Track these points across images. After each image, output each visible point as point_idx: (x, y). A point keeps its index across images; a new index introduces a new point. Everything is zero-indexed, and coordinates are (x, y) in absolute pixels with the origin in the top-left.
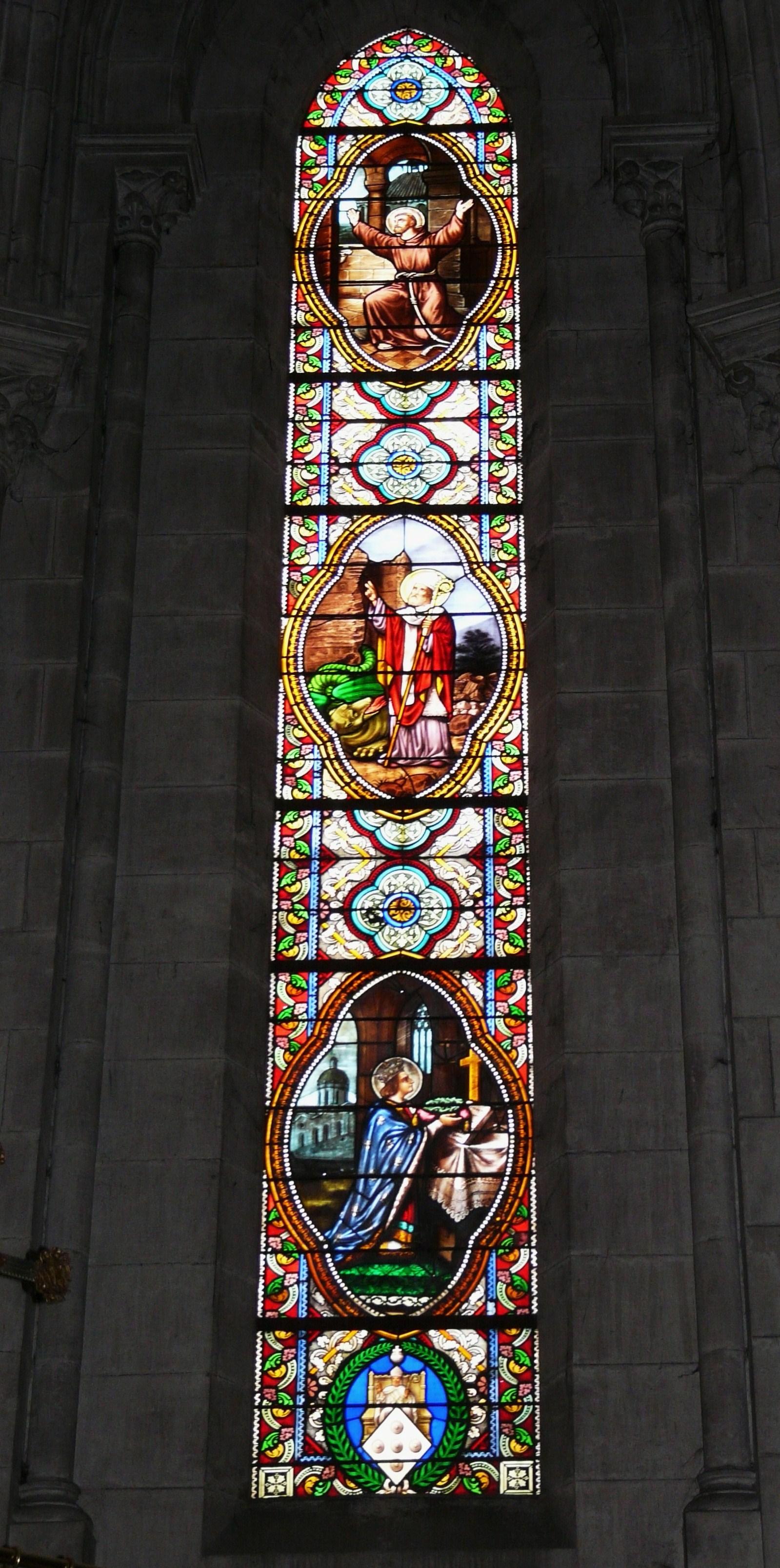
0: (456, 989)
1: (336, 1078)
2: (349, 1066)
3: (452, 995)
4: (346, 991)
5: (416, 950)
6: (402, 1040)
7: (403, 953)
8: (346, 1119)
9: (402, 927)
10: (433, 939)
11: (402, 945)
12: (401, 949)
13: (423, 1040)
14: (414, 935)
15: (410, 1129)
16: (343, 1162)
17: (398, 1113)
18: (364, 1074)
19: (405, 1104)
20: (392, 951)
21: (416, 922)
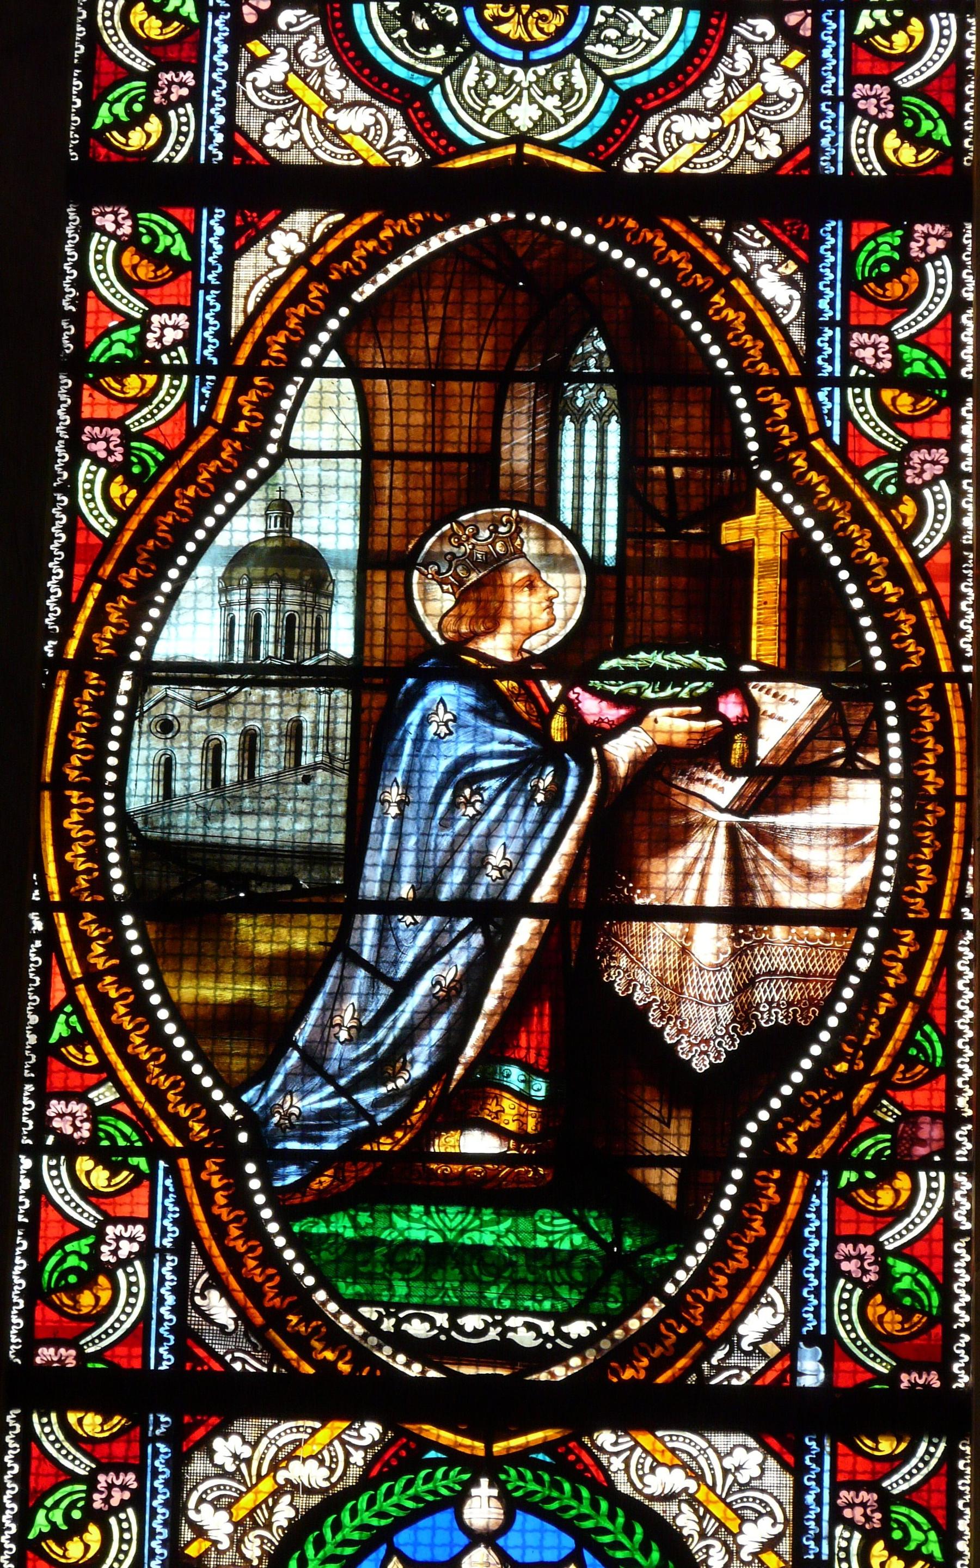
0: (714, 281)
1: (289, 562)
2: (331, 523)
3: (698, 302)
4: (322, 273)
6: (518, 452)
7: (529, 150)
8: (325, 714)
9: (526, 64)
10: (635, 107)
11: (524, 124)
12: (521, 139)
13: (591, 455)
14: (567, 93)
15: (545, 753)
16: (315, 855)
17: (499, 693)
18: (384, 559)
19: (526, 668)
20: (490, 144)
21: (577, 48)
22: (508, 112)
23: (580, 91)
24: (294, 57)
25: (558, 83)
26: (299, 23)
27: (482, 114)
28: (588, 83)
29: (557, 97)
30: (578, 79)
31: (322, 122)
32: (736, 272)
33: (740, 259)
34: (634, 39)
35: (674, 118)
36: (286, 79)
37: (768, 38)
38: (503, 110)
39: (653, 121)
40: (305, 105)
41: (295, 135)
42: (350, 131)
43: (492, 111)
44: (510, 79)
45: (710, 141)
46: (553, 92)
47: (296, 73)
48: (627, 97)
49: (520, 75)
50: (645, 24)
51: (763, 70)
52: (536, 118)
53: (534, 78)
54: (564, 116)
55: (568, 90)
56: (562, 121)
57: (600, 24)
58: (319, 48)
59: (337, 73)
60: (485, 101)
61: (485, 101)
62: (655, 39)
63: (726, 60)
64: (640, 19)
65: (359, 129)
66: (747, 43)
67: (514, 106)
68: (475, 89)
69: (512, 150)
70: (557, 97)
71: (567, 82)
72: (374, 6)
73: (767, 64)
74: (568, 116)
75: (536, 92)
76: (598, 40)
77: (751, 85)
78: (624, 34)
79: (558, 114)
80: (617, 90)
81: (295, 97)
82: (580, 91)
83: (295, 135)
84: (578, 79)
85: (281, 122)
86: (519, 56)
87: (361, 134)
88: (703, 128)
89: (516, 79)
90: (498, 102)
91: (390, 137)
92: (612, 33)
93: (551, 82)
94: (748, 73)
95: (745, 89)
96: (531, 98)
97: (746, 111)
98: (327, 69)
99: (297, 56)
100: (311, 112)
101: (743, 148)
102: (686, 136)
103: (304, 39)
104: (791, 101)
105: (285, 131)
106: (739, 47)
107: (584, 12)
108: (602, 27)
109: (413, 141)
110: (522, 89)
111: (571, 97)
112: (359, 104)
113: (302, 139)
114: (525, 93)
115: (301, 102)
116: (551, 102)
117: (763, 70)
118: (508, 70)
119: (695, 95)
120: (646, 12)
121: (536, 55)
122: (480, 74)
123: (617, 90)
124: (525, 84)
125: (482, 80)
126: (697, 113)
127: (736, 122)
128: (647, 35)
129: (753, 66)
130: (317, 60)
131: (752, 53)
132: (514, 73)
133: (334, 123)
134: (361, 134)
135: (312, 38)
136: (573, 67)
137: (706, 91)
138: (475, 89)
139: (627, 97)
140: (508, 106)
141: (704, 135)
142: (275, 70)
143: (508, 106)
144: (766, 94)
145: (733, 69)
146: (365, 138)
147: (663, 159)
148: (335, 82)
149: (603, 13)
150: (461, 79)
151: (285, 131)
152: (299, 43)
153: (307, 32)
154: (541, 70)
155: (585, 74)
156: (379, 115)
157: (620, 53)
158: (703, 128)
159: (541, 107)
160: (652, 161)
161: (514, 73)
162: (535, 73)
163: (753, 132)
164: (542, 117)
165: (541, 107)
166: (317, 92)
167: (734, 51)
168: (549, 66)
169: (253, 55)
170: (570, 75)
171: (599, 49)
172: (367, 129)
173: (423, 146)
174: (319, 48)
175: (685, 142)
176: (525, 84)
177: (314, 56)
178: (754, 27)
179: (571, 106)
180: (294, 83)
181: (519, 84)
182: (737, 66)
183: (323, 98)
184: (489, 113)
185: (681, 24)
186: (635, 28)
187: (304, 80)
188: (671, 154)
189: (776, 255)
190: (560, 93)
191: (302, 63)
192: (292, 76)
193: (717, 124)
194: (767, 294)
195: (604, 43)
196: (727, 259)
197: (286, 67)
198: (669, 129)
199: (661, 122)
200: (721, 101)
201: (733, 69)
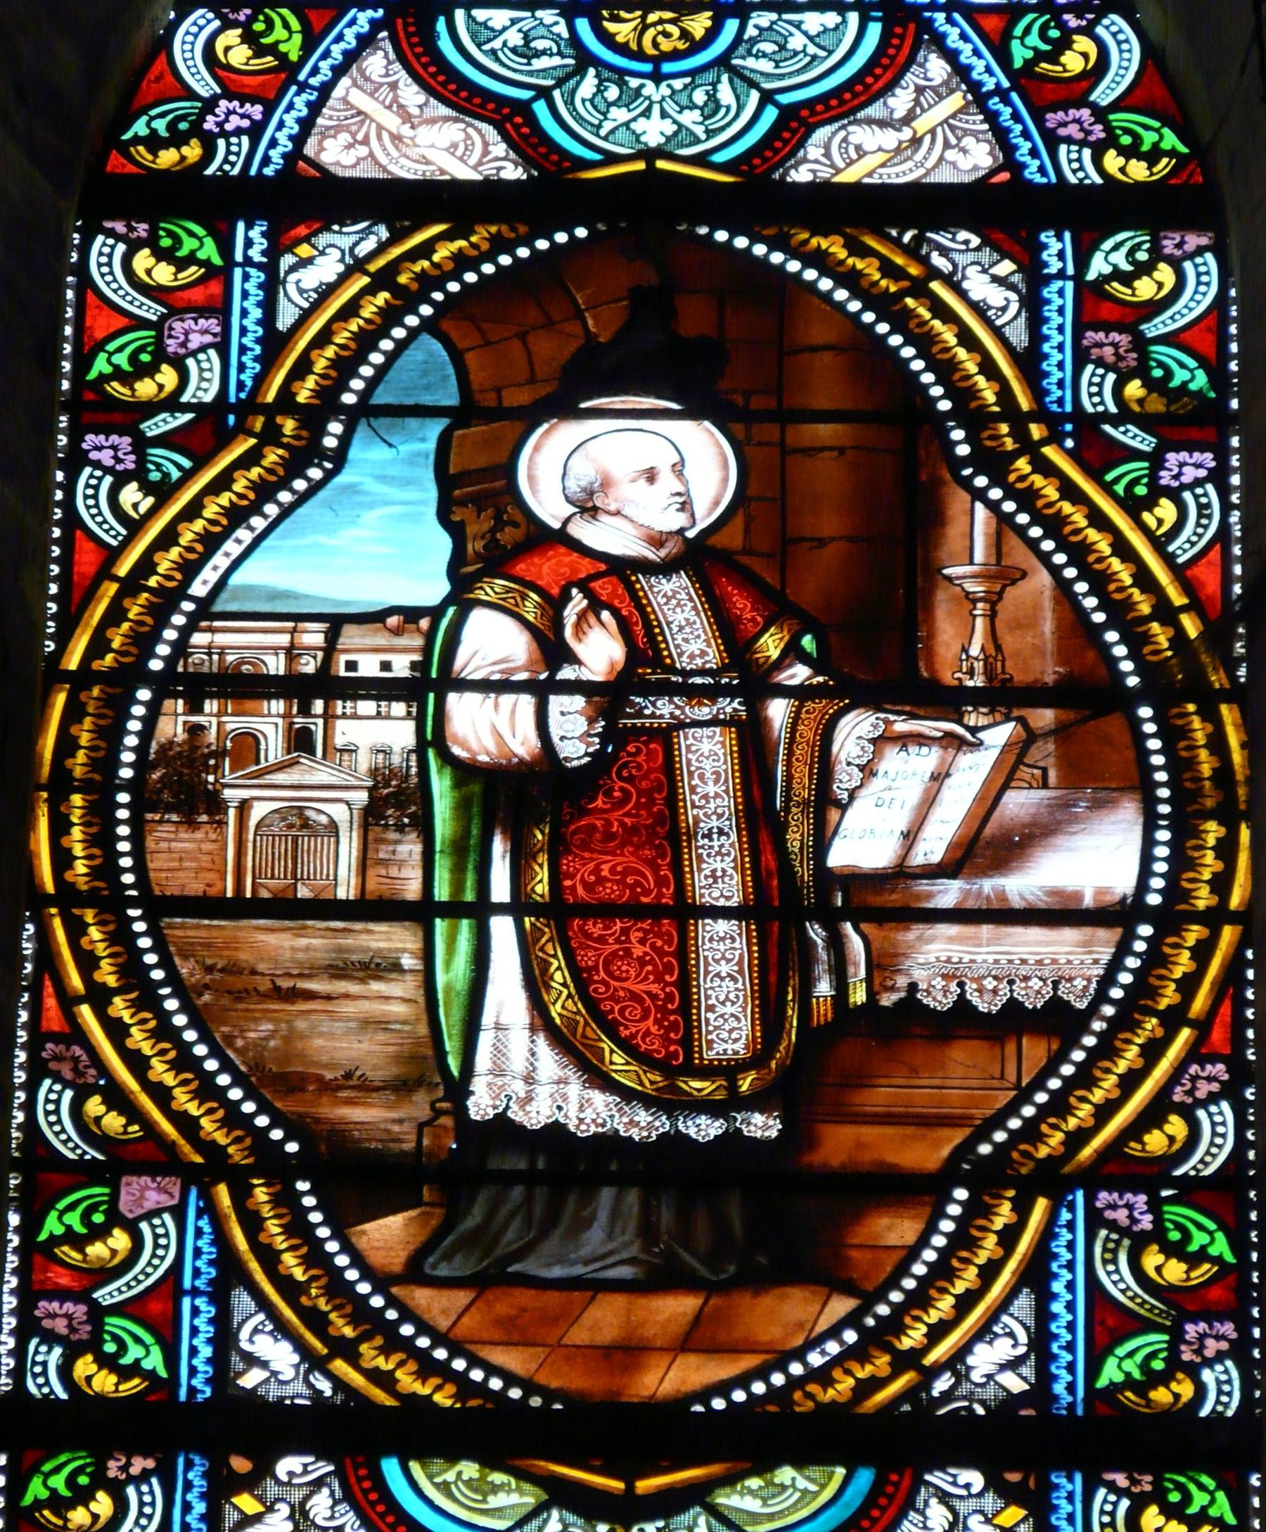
5: (719, 158)
7: (661, 164)
9: (657, 77)
12: (649, 155)
14: (712, 106)
21: (723, 61)
22: (633, 125)
23: (728, 108)
25: (699, 97)
27: (599, 127)
28: (738, 98)
29: (698, 112)
30: (725, 94)
32: (935, 273)
33: (937, 260)
34: (796, 53)
35: (850, 128)
38: (627, 124)
39: (821, 134)
40: (372, 120)
41: (362, 151)
42: (432, 146)
43: (614, 124)
44: (638, 92)
46: (693, 106)
48: (787, 113)
49: (650, 88)
50: (811, 39)
52: (669, 133)
53: (668, 92)
54: (707, 131)
55: (711, 105)
56: (703, 136)
57: (751, 38)
58: (390, 63)
59: (415, 88)
60: (604, 114)
61: (604, 114)
62: (824, 54)
64: (805, 33)
67: (642, 120)
68: (592, 101)
69: (640, 166)
70: (698, 112)
71: (712, 97)
72: (460, 15)
74: (710, 133)
75: (670, 107)
76: (749, 53)
78: (782, 48)
79: (699, 131)
80: (777, 104)
82: (728, 108)
83: (362, 151)
84: (725, 94)
85: (344, 138)
86: (647, 67)
87: (447, 150)
89: (645, 92)
90: (620, 115)
91: (486, 152)
92: (769, 47)
93: (690, 97)
96: (664, 115)
97: (946, 121)
98: (401, 85)
100: (380, 128)
102: (866, 147)
105: (349, 146)
107: (731, 26)
108: (753, 41)
109: (512, 155)
110: (651, 103)
111: (715, 112)
113: (371, 154)
114: (656, 109)
116: (690, 118)
118: (634, 83)
119: (878, 105)
120: (814, 21)
121: (667, 67)
122: (598, 86)
123: (777, 104)
124: (656, 98)
125: (600, 90)
126: (882, 124)
127: (933, 132)
128: (812, 49)
132: (642, 86)
134: (447, 150)
136: (719, 81)
138: (592, 101)
139: (787, 113)
140: (634, 119)
143: (634, 119)
148: (412, 95)
149: (756, 26)
150: (573, 92)
151: (349, 146)
154: (678, 84)
155: (734, 90)
156: (470, 130)
157: (777, 67)
159: (675, 122)
160: (825, 173)
161: (642, 86)
162: (669, 86)
164: (676, 134)
165: (675, 122)
168: (688, 80)
170: (715, 90)
171: (750, 62)
173: (526, 159)
174: (390, 63)
176: (656, 98)
179: (715, 123)
181: (648, 98)
182: (930, 75)
183: (398, 114)
184: (607, 126)
185: (853, 40)
186: (797, 41)
187: (372, 95)
188: (848, 165)
189: (986, 255)
190: (702, 109)
191: (367, 79)
194: (975, 296)
195: (757, 57)
196: (925, 261)
199: (834, 134)
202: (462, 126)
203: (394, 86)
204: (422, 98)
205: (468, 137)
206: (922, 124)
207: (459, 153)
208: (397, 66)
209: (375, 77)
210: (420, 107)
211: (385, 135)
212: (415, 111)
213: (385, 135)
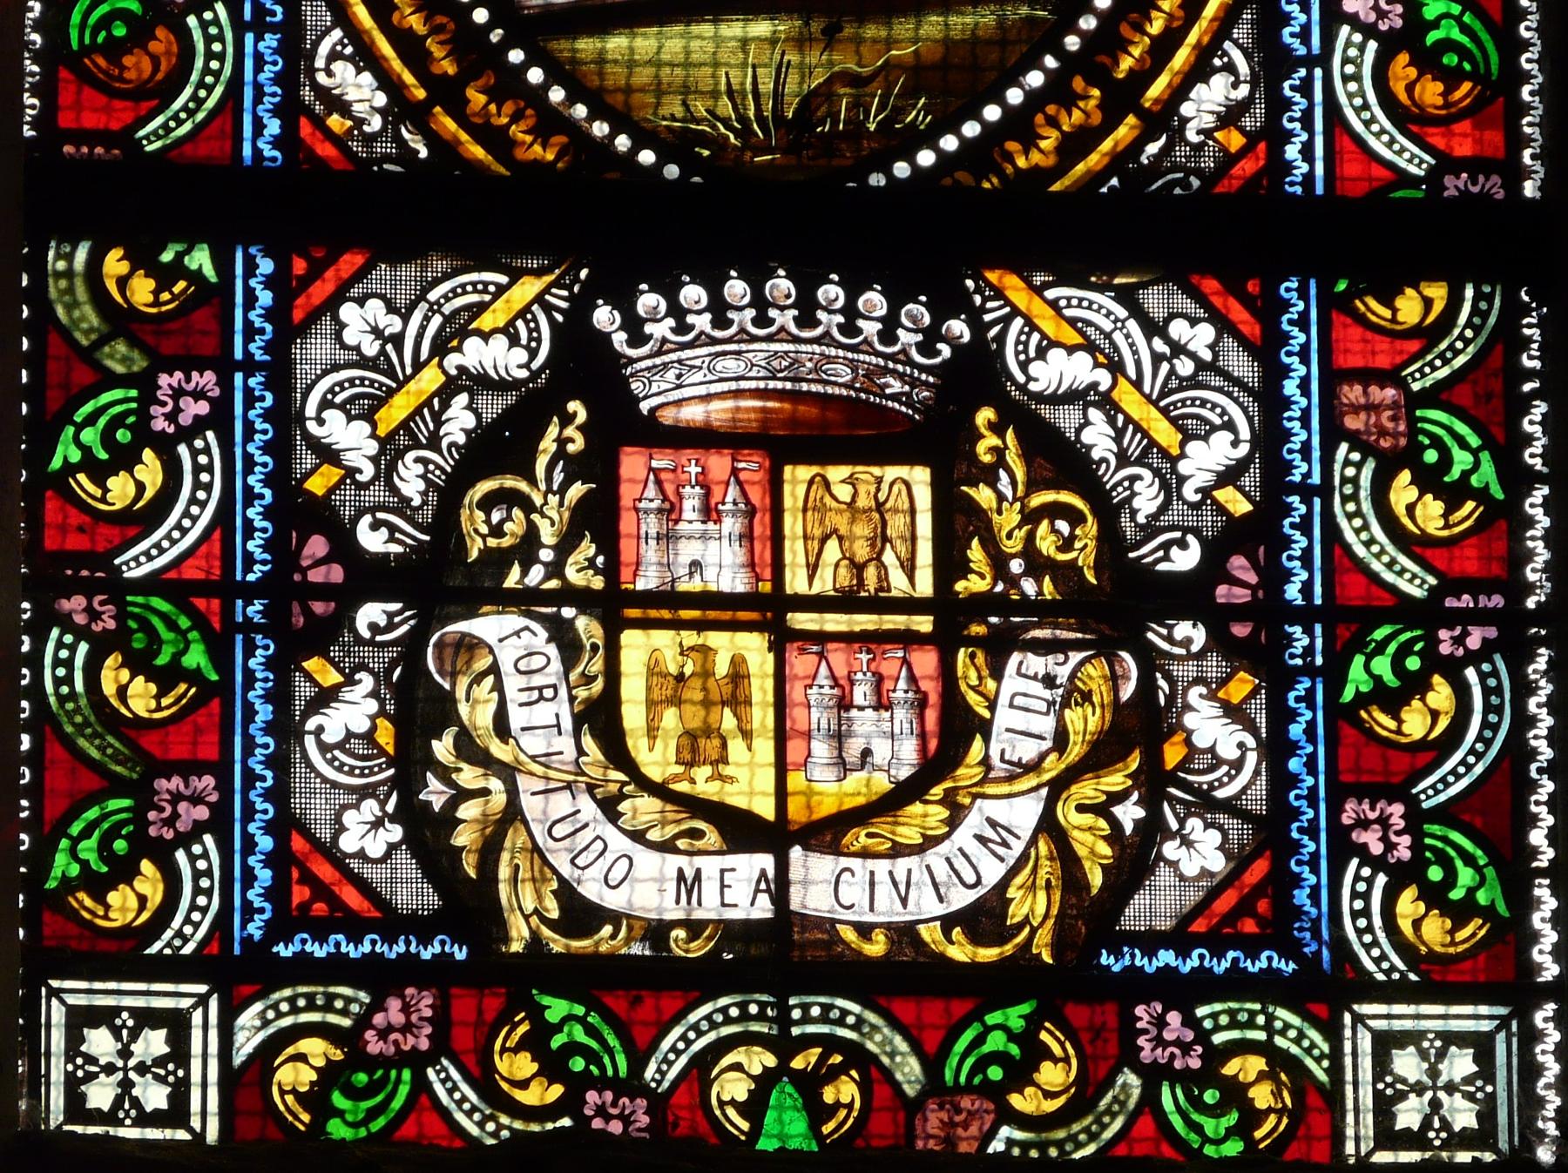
24: (1170, 485)
26: (1166, 546)
31: (1116, 368)
35: (524, 374)
36: (1182, 445)
37: (367, 520)
40: (1148, 397)
45: (464, 333)
47: (1164, 453)
51: (375, 460)
63: (438, 478)
65: (1055, 354)
66: (403, 506)
73: (368, 471)
77: (395, 432)
81: (1165, 412)
88: (475, 354)
94: (400, 454)
95: (404, 425)
99: (1165, 486)
100: (1137, 384)
101: (406, 319)
102: (500, 341)
103: (1154, 517)
104: (325, 404)
106: (417, 502)
112: (1056, 399)
115: (1155, 404)
117: (375, 460)
119: (488, 415)
127: (418, 366)
129: (392, 468)
130: (1133, 479)
131: (394, 491)
133: (1097, 365)
135: (1141, 519)
137: (470, 421)
141: (472, 343)
142: (1205, 460)
144: (369, 416)
145: (425, 462)
146: (1044, 336)
147: (539, 299)
148: (1098, 438)
152: (1164, 508)
153: (1150, 530)
158: (475, 354)
163: (389, 347)
166: (1128, 419)
167: (424, 494)
169: (1240, 489)
172: (1041, 354)
175: (503, 330)
177: (1138, 486)
178: (391, 539)
180: (1166, 435)
182: (420, 469)
183: (1119, 410)
187: (1153, 443)
188: (527, 309)
191: (1157, 472)
192: (1175, 451)
193: (452, 361)
197: (1184, 467)
198: (533, 354)
200: (446, 405)
201: (425, 462)
202: (1033, 387)
203: (1123, 459)
204: (1087, 436)
205: (1024, 366)
206: (431, 379)
207: (1036, 337)
208: (1120, 495)
209: (1147, 474)
210: (1087, 423)
211: (1131, 371)
212: (1095, 414)
213: (1131, 371)
